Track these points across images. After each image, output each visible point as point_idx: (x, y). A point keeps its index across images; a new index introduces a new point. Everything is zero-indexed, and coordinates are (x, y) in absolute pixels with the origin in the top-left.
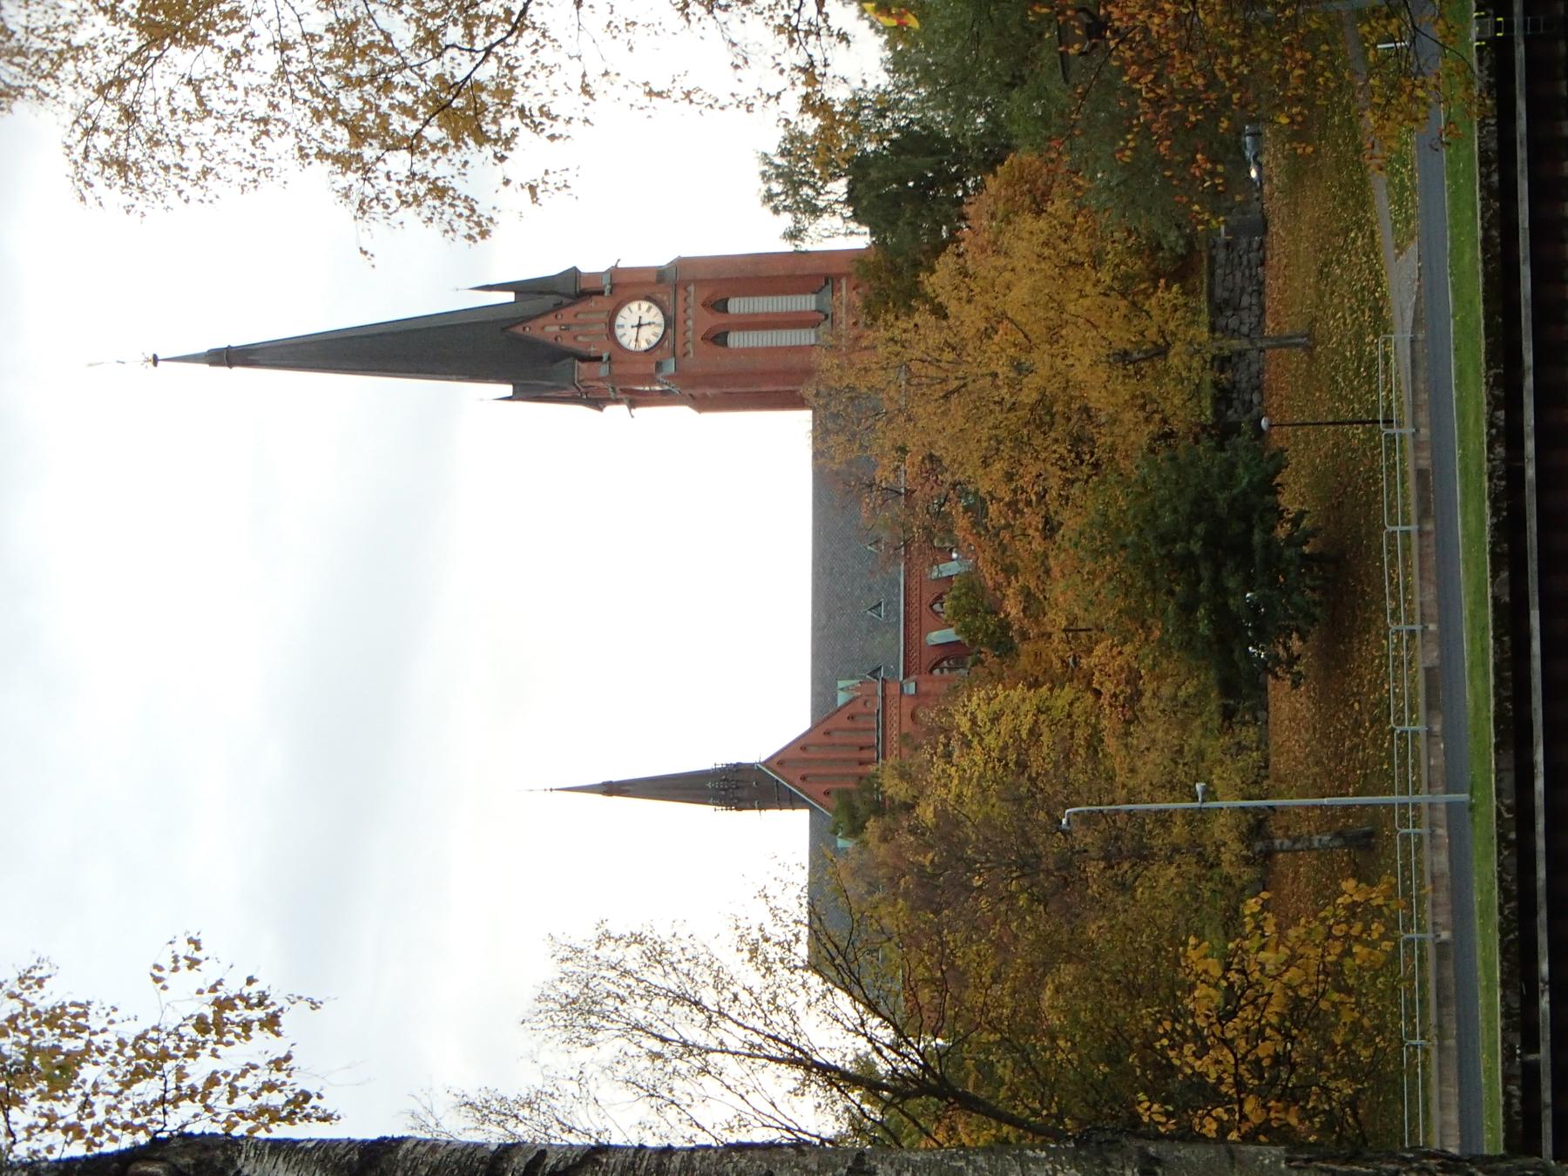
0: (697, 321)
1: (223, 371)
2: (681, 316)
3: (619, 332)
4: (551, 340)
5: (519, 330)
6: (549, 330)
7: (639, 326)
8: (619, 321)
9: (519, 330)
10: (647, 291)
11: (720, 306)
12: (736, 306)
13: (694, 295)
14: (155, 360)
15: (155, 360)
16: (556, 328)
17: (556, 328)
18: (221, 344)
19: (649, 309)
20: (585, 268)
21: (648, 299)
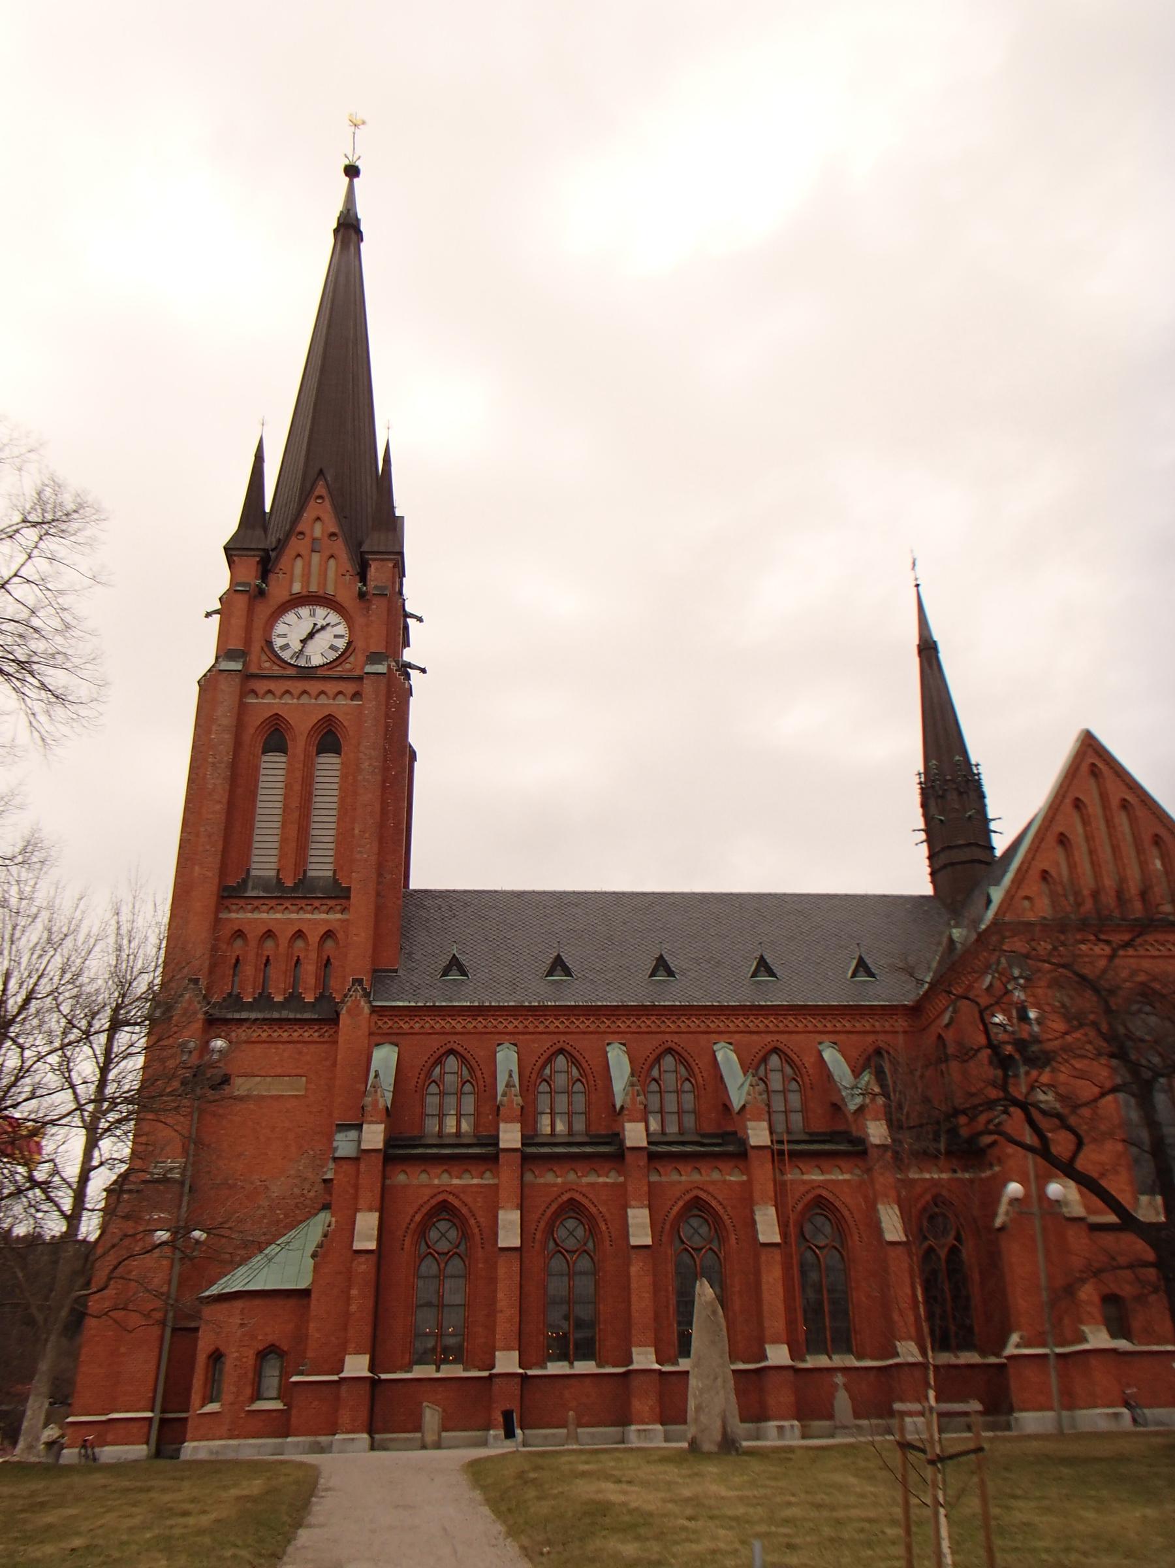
2: (314, 687)
10: (359, 644)
11: (328, 738)
13: (341, 707)
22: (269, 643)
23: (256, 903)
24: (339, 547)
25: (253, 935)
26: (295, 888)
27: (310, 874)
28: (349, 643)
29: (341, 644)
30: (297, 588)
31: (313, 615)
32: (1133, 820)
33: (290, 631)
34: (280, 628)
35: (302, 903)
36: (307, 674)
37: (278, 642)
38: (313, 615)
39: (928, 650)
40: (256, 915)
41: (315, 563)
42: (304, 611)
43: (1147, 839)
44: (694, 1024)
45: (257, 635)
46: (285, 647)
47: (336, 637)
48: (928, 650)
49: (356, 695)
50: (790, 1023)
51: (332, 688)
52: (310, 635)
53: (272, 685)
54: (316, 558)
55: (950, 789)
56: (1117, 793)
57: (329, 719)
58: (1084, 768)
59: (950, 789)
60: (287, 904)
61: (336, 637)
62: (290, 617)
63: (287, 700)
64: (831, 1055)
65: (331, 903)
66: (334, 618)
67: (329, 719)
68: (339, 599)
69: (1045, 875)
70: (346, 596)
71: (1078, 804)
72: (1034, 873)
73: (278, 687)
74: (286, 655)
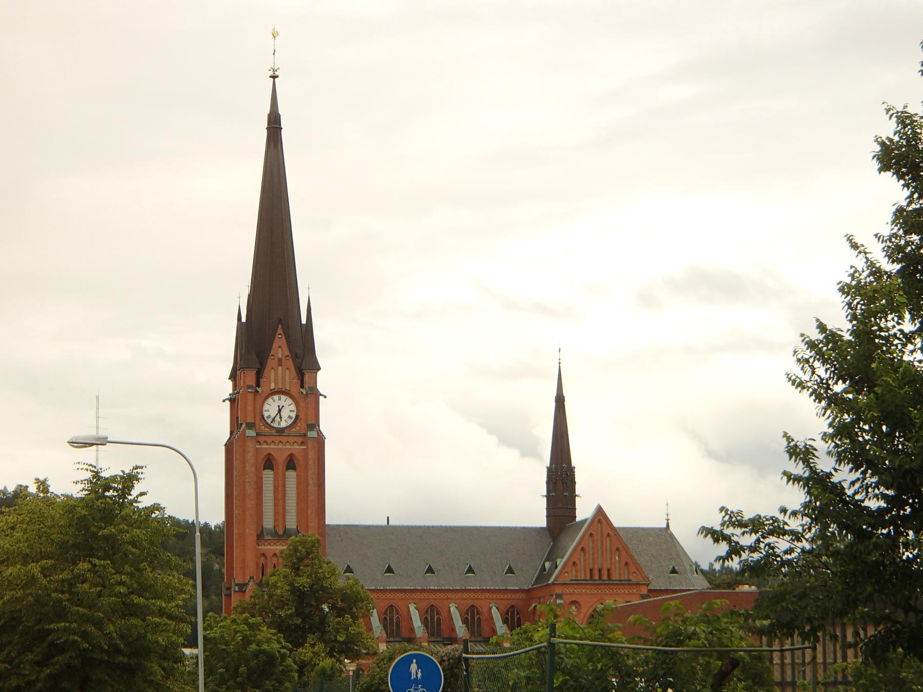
0: (280, 450)
1: (265, 124)
2: (284, 439)
5: (280, 330)
6: (280, 349)
7: (280, 411)
9: (280, 330)
10: (302, 416)
11: (291, 464)
12: (291, 475)
14: (274, 77)
15: (274, 77)
19: (290, 417)
22: (263, 416)
25: (269, 555)
26: (283, 536)
28: (297, 417)
29: (293, 415)
30: (273, 386)
31: (280, 399)
32: (611, 541)
33: (270, 408)
34: (266, 407)
36: (280, 431)
37: (266, 414)
38: (280, 399)
39: (560, 401)
40: (269, 547)
41: (279, 372)
42: (276, 397)
43: (614, 549)
44: (442, 595)
45: (258, 412)
46: (269, 417)
48: (560, 401)
49: (302, 443)
50: (480, 596)
51: (291, 440)
52: (279, 410)
53: (266, 439)
54: (280, 368)
55: (561, 480)
56: (607, 530)
57: (291, 455)
58: (596, 520)
59: (561, 480)
62: (270, 401)
63: (272, 446)
64: (494, 610)
66: (289, 401)
67: (291, 455)
69: (574, 563)
70: (294, 392)
71: (591, 535)
72: (571, 563)
73: (269, 440)
74: (269, 421)
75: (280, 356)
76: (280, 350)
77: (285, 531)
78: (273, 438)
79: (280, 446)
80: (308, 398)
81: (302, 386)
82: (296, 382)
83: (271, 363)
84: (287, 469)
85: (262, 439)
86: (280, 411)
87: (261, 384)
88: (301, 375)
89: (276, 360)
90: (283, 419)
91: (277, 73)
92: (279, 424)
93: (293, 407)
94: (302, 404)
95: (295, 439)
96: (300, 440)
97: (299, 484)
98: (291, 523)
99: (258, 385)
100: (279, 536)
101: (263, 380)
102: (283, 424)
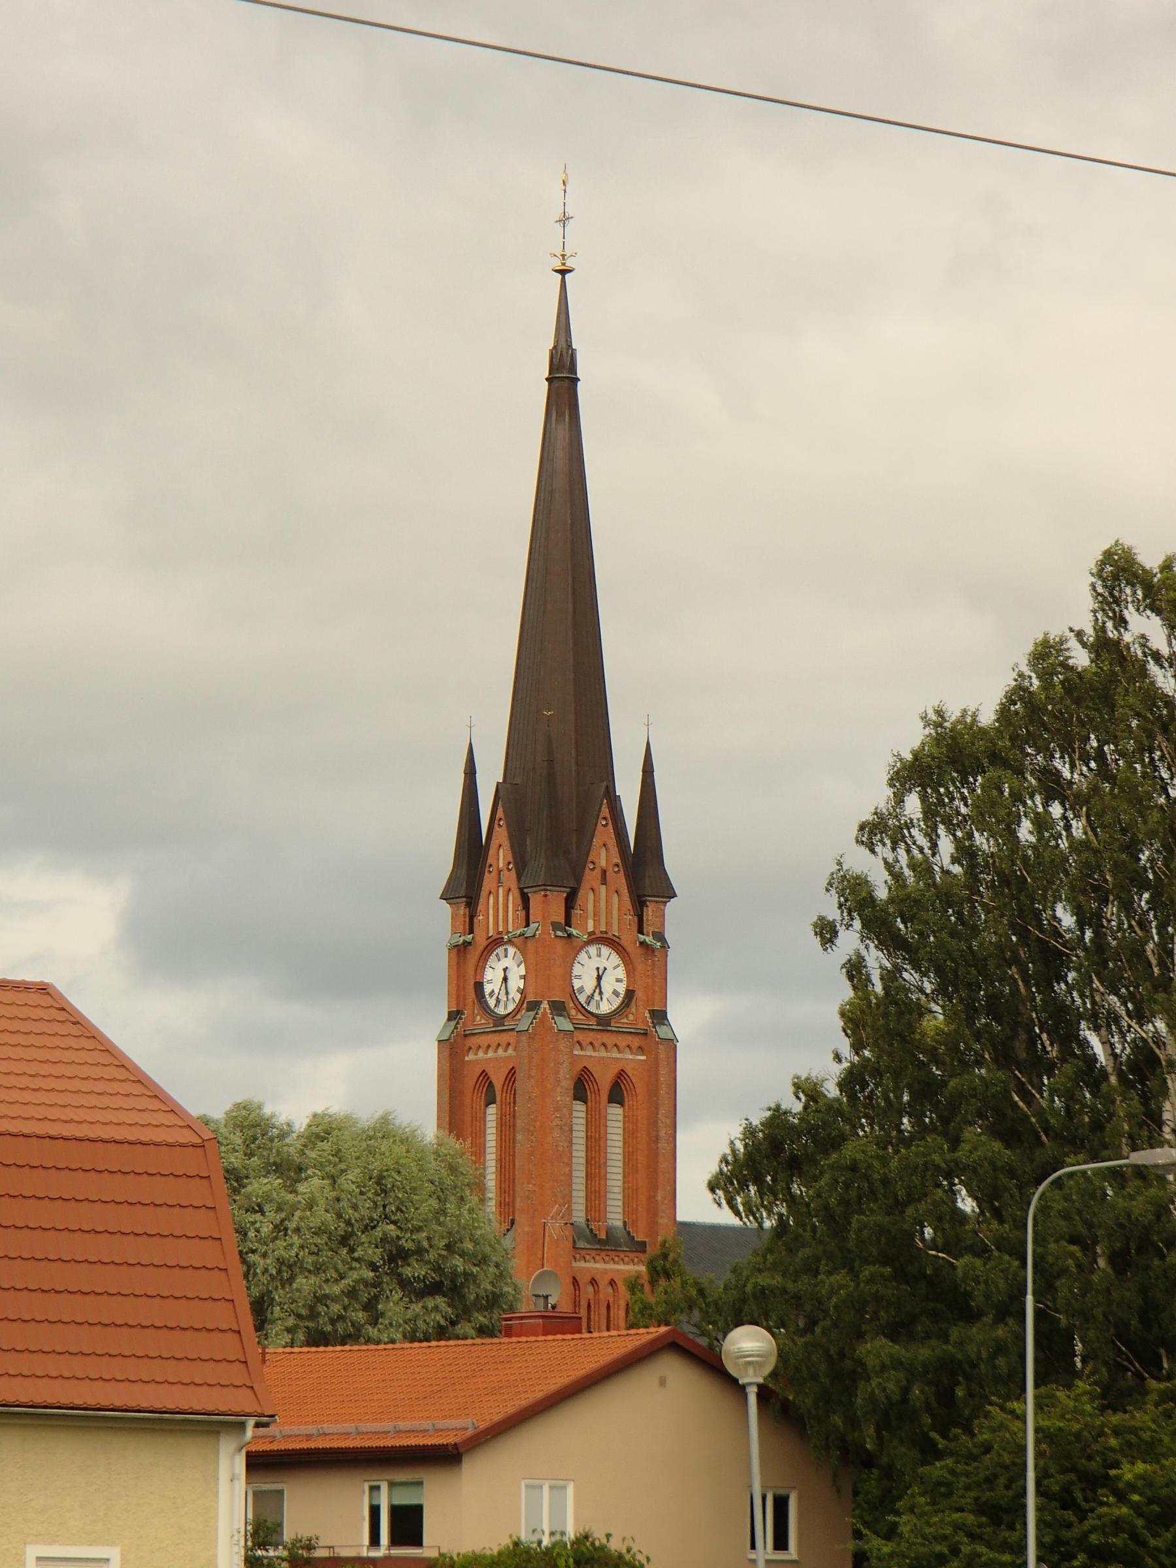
0: (608, 1058)
2: (609, 1039)
3: (593, 950)
4: (590, 859)
7: (599, 978)
8: (605, 951)
10: (640, 994)
12: (615, 1113)
13: (631, 1060)
14: (563, 272)
15: (563, 272)
16: (603, 863)
17: (603, 863)
18: (583, 370)
20: (671, 907)
21: (630, 994)
23: (583, 1253)
24: (620, 881)
27: (610, 1222)
29: (622, 988)
35: (613, 1254)
36: (604, 1021)
46: (581, 990)
47: (618, 980)
51: (623, 1041)
60: (603, 1254)
61: (618, 980)
62: (582, 957)
65: (632, 1255)
66: (615, 959)
67: (622, 1074)
68: (624, 943)
74: (582, 999)
75: (603, 863)
76: (603, 852)
77: (609, 1231)
78: (591, 1036)
79: (603, 1053)
80: (647, 955)
81: (641, 931)
82: (630, 918)
83: (591, 878)
84: (610, 1102)
85: (579, 1036)
86: (599, 978)
87: (573, 921)
88: (639, 904)
89: (598, 872)
90: (604, 997)
91: (570, 263)
92: (598, 1007)
93: (621, 973)
94: (640, 968)
95: (629, 1039)
96: (636, 1042)
97: (629, 1134)
98: (615, 1217)
99: (568, 923)
100: (600, 1241)
101: (577, 912)
102: (605, 1008)
